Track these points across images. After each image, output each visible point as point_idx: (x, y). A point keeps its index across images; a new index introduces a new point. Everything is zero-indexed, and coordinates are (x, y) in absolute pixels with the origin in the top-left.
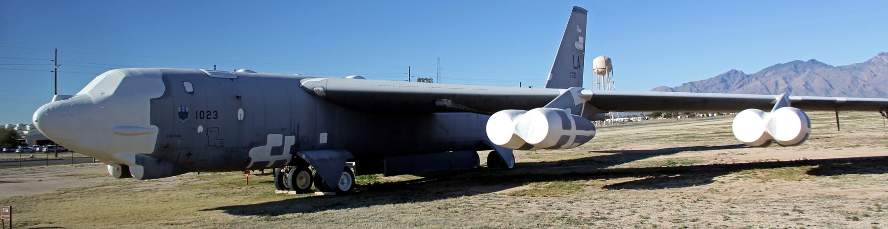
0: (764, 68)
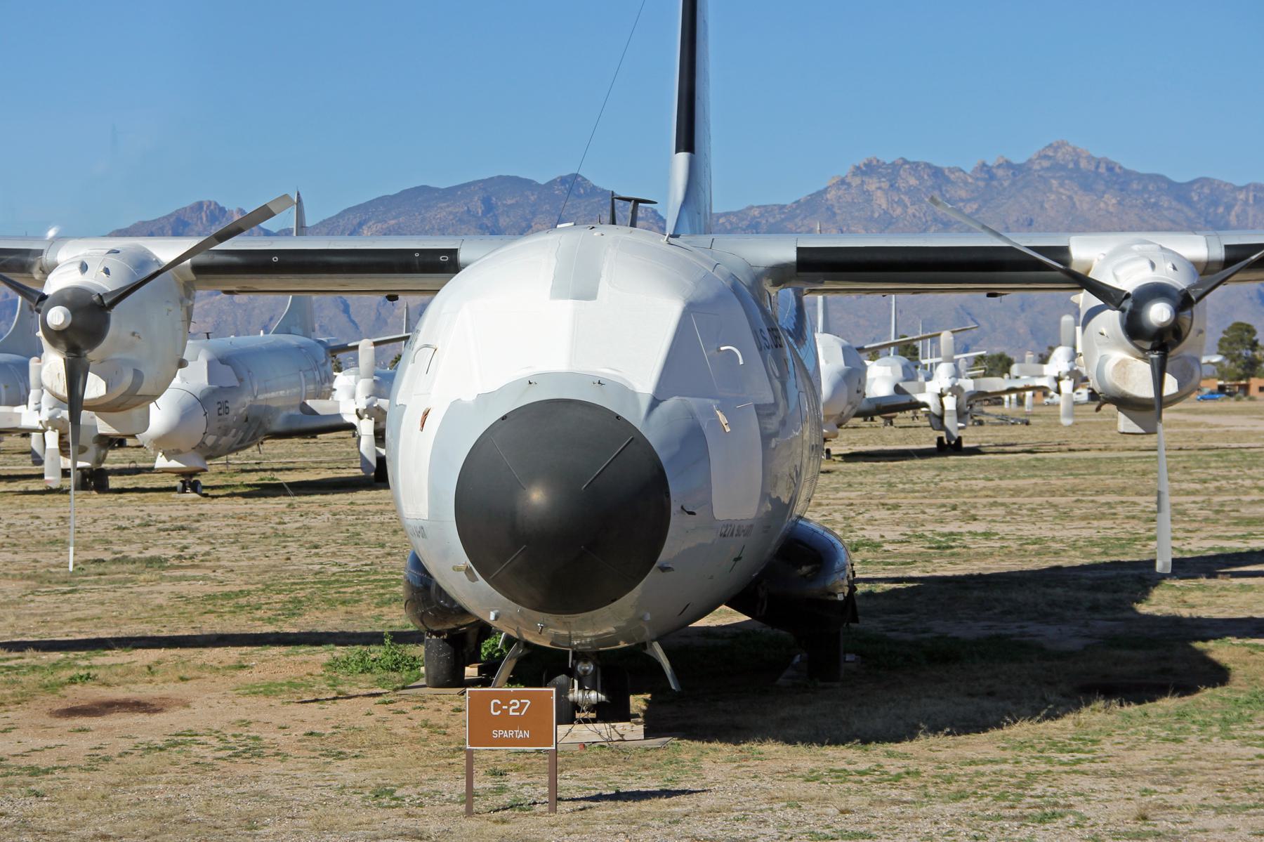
0: (345, 207)
